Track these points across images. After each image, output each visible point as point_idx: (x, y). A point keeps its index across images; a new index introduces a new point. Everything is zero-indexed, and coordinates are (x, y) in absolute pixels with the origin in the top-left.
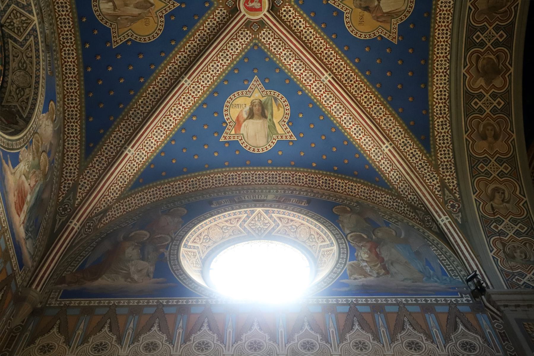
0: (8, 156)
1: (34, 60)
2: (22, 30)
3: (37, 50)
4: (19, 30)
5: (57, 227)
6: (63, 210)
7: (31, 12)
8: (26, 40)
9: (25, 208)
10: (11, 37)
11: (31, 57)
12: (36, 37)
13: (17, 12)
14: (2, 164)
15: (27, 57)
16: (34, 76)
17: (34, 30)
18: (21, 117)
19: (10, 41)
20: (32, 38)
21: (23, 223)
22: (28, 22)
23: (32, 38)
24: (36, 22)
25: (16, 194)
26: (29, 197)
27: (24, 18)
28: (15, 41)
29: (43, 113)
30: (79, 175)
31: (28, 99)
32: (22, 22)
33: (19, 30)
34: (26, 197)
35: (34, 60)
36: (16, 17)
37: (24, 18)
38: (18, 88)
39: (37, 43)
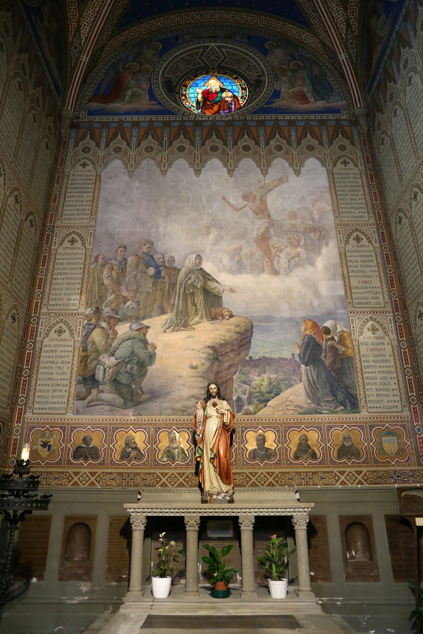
0: (271, 100)
1: (236, 52)
2: (217, 55)
3: (230, 48)
4: (217, 57)
5: (339, 69)
6: (333, 59)
7: (208, 47)
8: (223, 54)
9: (309, 95)
10: (220, 63)
11: (233, 53)
12: (223, 47)
13: (206, 56)
14: (271, 108)
15: (233, 56)
16: (244, 55)
17: (218, 47)
18: (260, 76)
19: (222, 64)
20: (223, 49)
21: (316, 100)
22: (213, 50)
23: (223, 49)
24: (214, 44)
25: (295, 101)
26: (305, 90)
27: (211, 52)
28: (223, 61)
29: (266, 56)
30: (318, 38)
31: (254, 66)
32: (213, 54)
33: (217, 57)
34: (303, 92)
35: (236, 52)
36: (209, 57)
37: (211, 52)
38: (247, 69)
39: (226, 47)
